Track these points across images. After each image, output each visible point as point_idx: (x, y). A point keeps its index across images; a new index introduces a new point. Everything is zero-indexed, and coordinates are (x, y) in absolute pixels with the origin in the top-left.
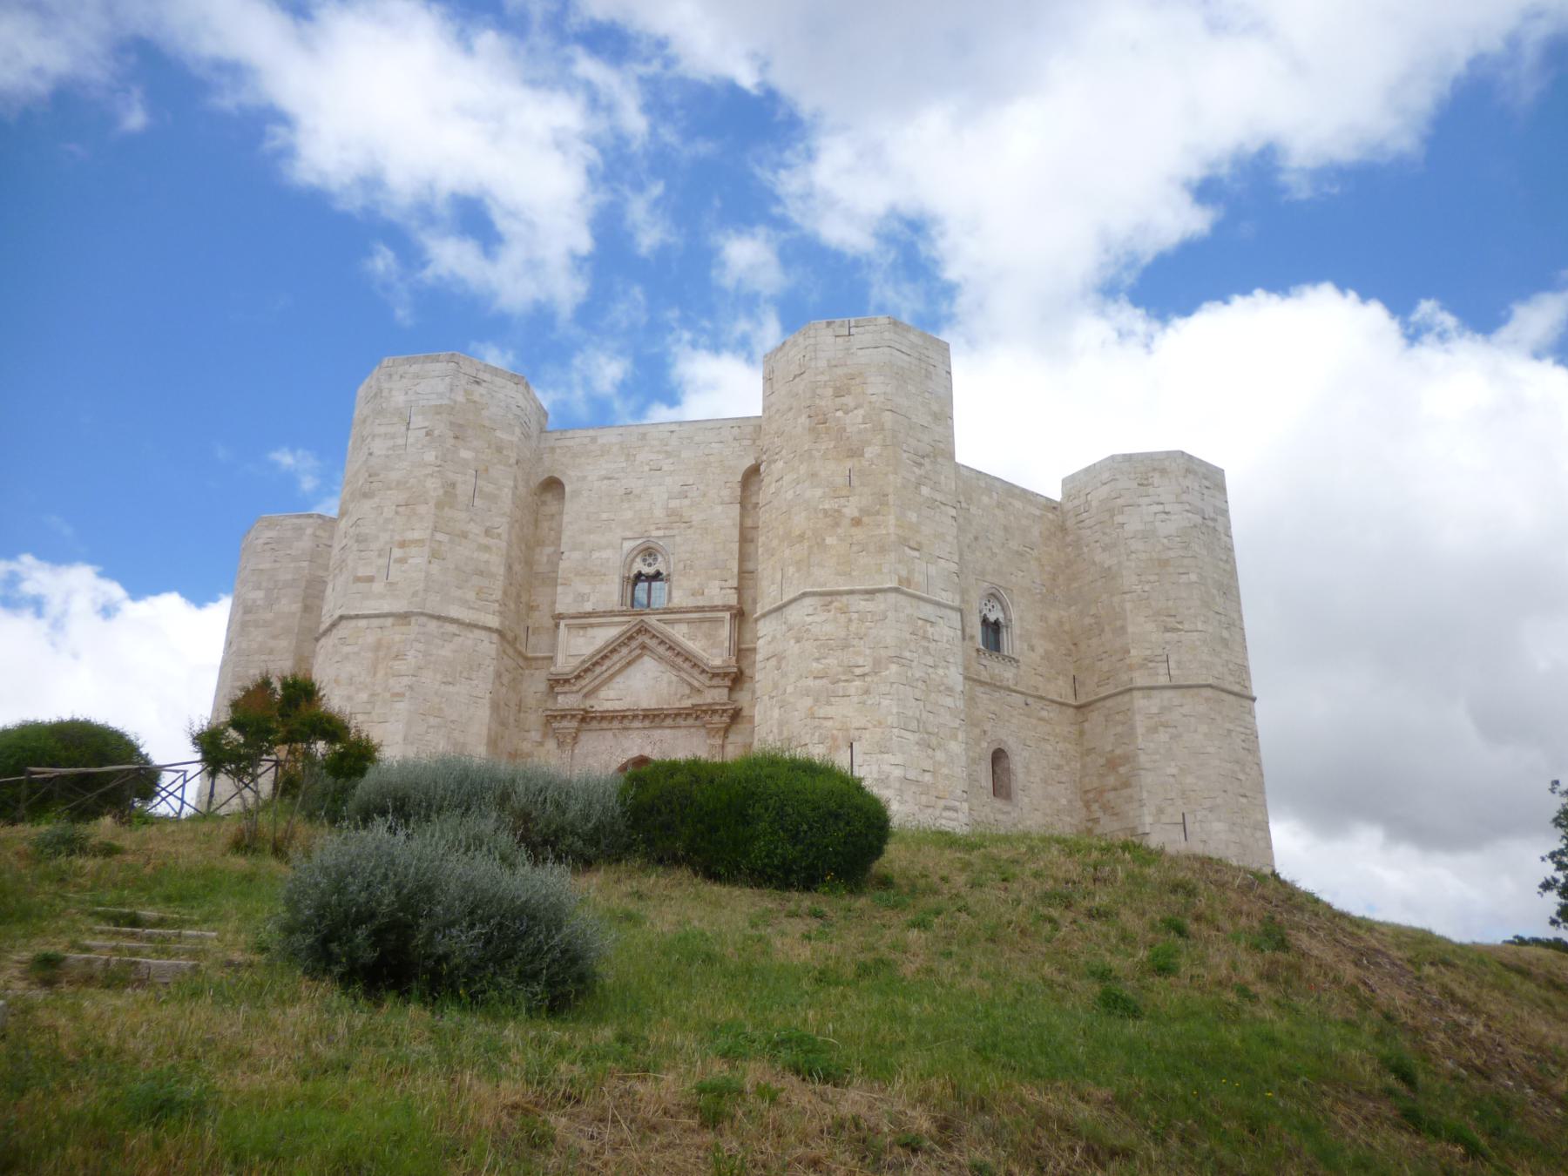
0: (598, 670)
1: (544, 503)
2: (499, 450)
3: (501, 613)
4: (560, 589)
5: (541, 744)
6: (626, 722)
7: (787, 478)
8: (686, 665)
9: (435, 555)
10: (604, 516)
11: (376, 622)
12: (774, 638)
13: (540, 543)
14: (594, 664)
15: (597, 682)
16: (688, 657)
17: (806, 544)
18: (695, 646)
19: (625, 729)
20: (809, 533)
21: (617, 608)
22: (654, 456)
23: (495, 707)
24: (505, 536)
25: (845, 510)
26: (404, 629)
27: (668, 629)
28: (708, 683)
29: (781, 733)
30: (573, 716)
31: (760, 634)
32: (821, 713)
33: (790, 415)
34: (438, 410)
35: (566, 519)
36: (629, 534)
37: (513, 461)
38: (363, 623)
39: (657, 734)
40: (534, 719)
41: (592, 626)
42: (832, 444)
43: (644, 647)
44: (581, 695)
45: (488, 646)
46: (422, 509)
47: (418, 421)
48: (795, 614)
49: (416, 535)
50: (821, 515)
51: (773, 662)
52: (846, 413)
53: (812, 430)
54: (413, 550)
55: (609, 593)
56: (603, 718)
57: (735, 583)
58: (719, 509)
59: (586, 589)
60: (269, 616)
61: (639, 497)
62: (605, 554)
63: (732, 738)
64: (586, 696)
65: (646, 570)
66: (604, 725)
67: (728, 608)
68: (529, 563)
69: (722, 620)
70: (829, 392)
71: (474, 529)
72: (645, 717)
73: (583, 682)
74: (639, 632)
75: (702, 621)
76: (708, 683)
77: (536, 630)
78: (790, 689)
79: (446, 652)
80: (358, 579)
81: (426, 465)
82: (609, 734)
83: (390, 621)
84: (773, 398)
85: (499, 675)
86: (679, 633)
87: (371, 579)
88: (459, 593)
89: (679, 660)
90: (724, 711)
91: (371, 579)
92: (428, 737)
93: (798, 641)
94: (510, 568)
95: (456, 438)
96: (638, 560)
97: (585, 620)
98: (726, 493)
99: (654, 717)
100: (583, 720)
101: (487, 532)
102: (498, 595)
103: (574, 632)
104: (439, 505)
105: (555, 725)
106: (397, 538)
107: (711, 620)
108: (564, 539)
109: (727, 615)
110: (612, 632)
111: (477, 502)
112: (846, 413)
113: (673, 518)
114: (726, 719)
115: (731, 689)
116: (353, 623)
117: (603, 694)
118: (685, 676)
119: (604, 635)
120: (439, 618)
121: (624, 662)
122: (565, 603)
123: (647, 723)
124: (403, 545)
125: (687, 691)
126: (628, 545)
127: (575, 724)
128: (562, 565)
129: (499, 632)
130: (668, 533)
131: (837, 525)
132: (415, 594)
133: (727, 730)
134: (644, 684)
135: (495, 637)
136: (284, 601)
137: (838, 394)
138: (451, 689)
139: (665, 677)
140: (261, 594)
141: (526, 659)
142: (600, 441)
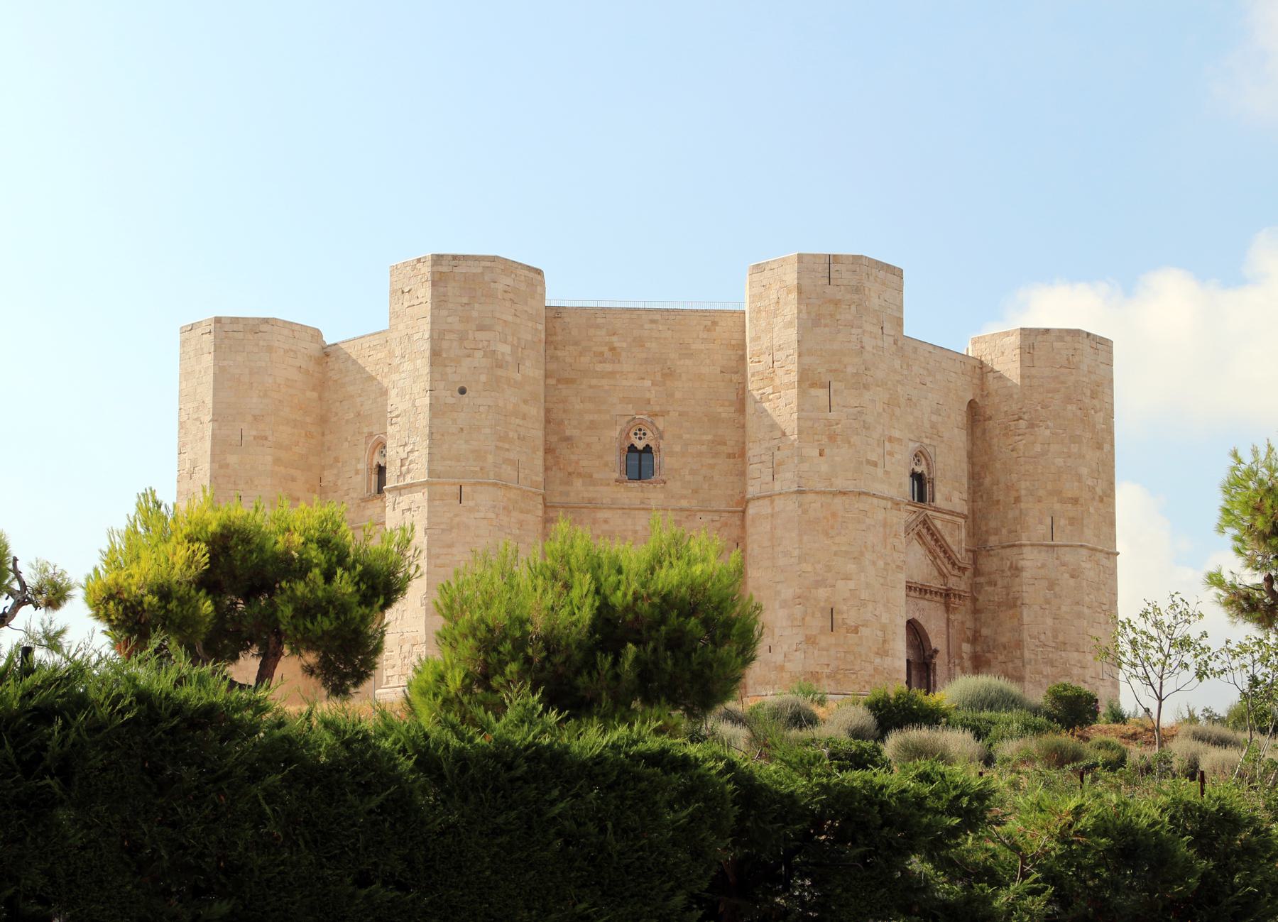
7: (1054, 447)
8: (942, 555)
11: (883, 503)
12: (1043, 566)
16: (946, 551)
18: (948, 539)
22: (921, 371)
29: (1055, 637)
32: (1092, 631)
36: (912, 437)
38: (875, 501)
48: (1068, 556)
53: (1082, 420)
57: (965, 496)
58: (956, 430)
60: (518, 377)
67: (965, 517)
69: (959, 527)
75: (948, 521)
78: (1064, 609)
80: (868, 462)
84: (1034, 371)
86: (938, 524)
87: (875, 464)
91: (875, 464)
93: (1072, 577)
98: (959, 418)
116: (870, 500)
124: (890, 439)
125: (936, 574)
131: (1093, 499)
136: (528, 363)
140: (507, 349)
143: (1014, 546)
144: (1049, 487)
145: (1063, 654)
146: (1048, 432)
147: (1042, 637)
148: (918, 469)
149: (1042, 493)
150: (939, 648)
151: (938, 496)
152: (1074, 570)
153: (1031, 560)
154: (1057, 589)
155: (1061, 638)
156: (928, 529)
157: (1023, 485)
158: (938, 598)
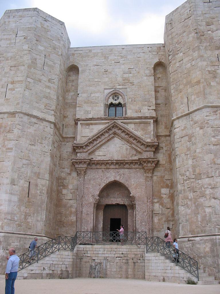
0: (95, 143)
1: (69, 76)
2: (54, 48)
3: (55, 116)
4: (78, 109)
5: (70, 174)
6: (108, 166)
8: (134, 142)
9: (27, 88)
10: (96, 80)
12: (185, 128)
13: (68, 91)
14: (93, 140)
15: (94, 148)
16: (135, 138)
17: (201, 85)
18: (138, 133)
19: (107, 168)
20: (202, 80)
21: (103, 117)
22: (116, 58)
23: (52, 157)
24: (56, 83)
25: (218, 71)
26: (13, 119)
27: (126, 126)
28: (145, 149)
29: (194, 171)
30: (85, 162)
31: (175, 127)
33: (185, 34)
34: (29, 29)
35: (80, 81)
37: (60, 54)
39: (122, 171)
40: (67, 164)
41: (92, 124)
42: (208, 44)
43: (115, 133)
44: (88, 153)
45: (50, 130)
46: (22, 68)
47: (20, 33)
48: (198, 117)
49: (19, 79)
50: (207, 73)
51: (187, 138)
52: (213, 32)
54: (17, 85)
55: (99, 111)
56: (98, 164)
58: (145, 78)
59: (89, 109)
61: (110, 73)
62: (97, 95)
63: (155, 174)
64: (90, 154)
65: (114, 102)
66: (98, 166)
67: (152, 118)
68: (64, 98)
70: (204, 23)
71: (44, 79)
72: (117, 163)
73: (89, 148)
74: (113, 127)
75: (140, 123)
76: (145, 149)
77: (67, 126)
78: (198, 151)
79: (32, 130)
81: (23, 50)
82: (100, 170)
83: (6, 115)
85: (53, 143)
88: (37, 105)
89: (131, 139)
90: (153, 162)
92: (23, 170)
93: (201, 128)
94: (58, 98)
95: (37, 41)
96: (111, 98)
97: (89, 121)
98: (147, 72)
99: (120, 164)
100: (89, 164)
101: (50, 81)
102: (54, 107)
103: (84, 127)
104: (29, 67)
105: (77, 166)
106: (10, 80)
107: (144, 123)
108: (79, 88)
109: (152, 121)
110: (101, 127)
111: (45, 68)
112: (213, 32)
113: (126, 81)
114: (153, 165)
115: (154, 152)
117: (97, 153)
118: (134, 146)
119: (97, 129)
120: (28, 115)
121: (106, 140)
122: (80, 114)
123: (117, 166)
125: (135, 153)
126: (107, 92)
127: (85, 166)
128: (79, 99)
129: (55, 124)
130: (123, 87)
132: (18, 104)
133: (153, 170)
134: (115, 149)
135: (52, 126)
137: (208, 24)
138: (33, 147)
139: (125, 147)
141: (63, 138)
142: (93, 51)
143: (172, 123)
144: (185, 81)
145: (200, 182)
146: (182, 54)
147: (188, 173)
148: (117, 102)
149: (181, 87)
150: (137, 195)
151: (128, 112)
152: (202, 123)
153: (179, 126)
154: (193, 139)
155: (197, 171)
156: (120, 129)
157: (172, 87)
158: (137, 166)
